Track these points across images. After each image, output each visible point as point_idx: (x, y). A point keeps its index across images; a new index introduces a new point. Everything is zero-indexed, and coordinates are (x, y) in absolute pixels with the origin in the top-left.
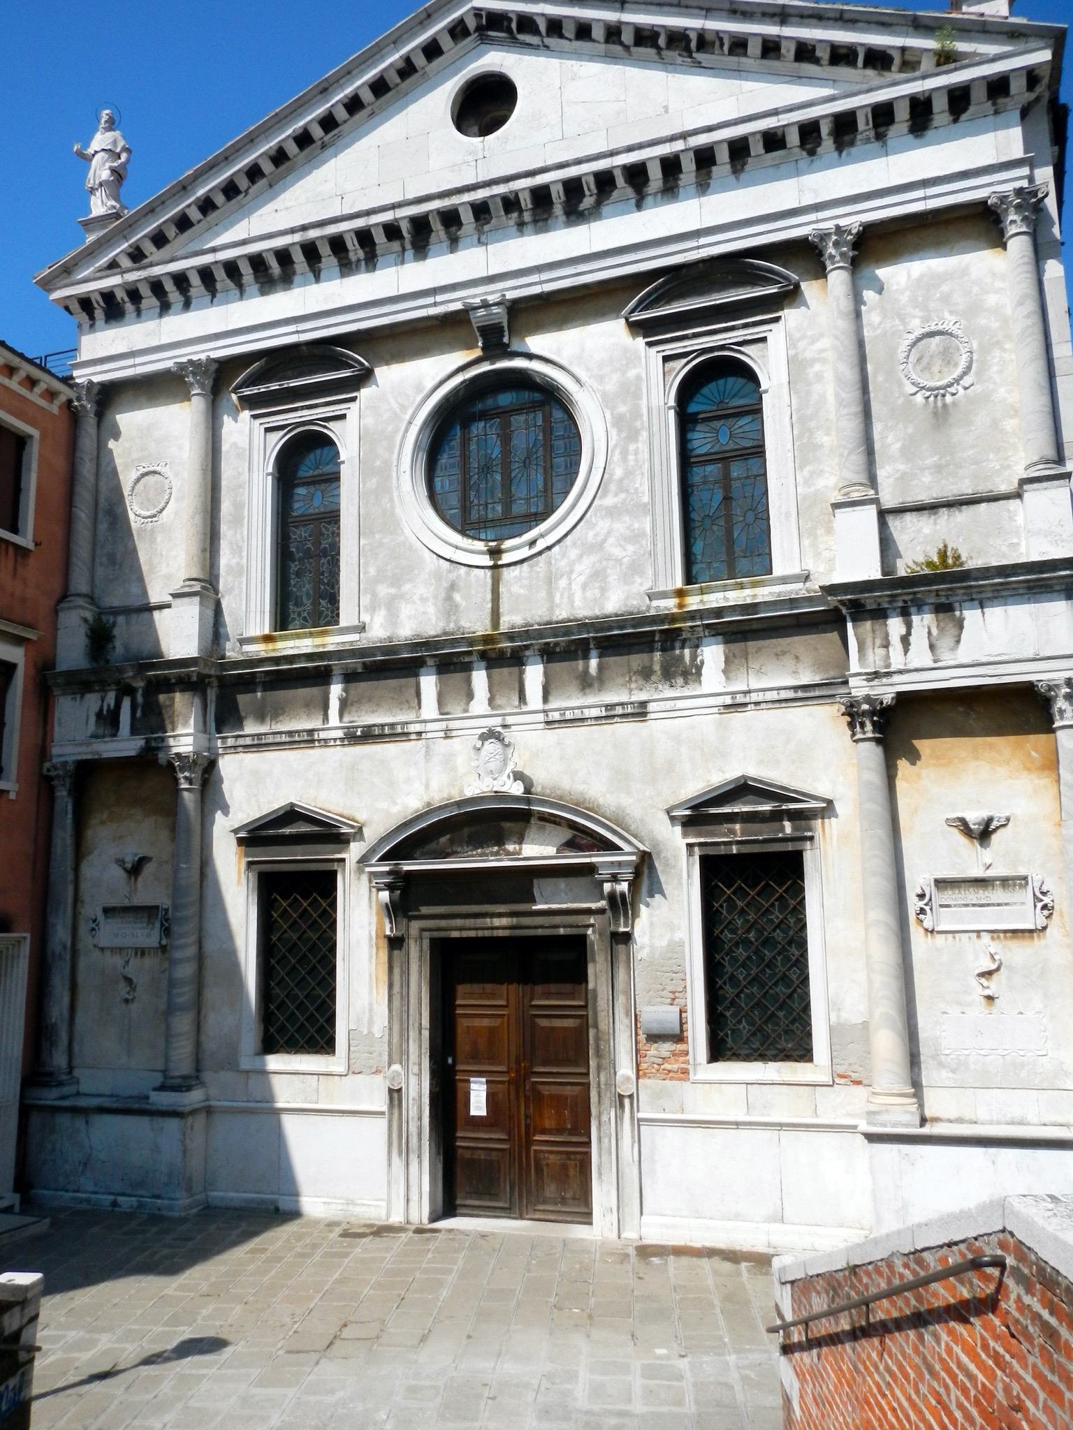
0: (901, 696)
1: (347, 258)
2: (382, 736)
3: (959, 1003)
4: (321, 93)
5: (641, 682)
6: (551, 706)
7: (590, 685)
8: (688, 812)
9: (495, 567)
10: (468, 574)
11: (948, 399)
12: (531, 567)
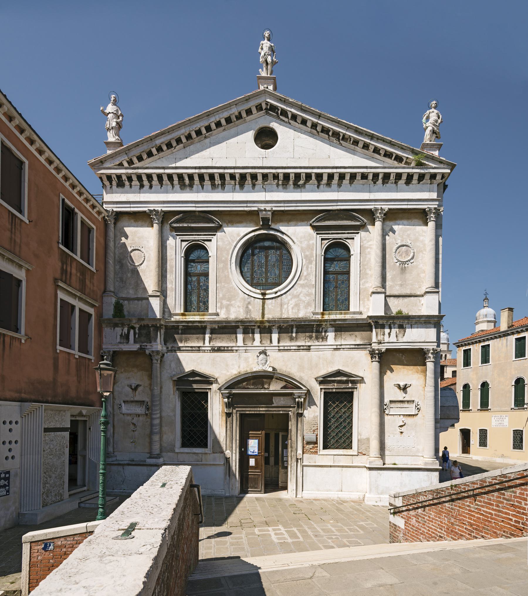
5: (309, 339)
6: (280, 345)
7: (293, 339)
9: (264, 299)
10: (254, 300)
11: (406, 265)
12: (275, 300)
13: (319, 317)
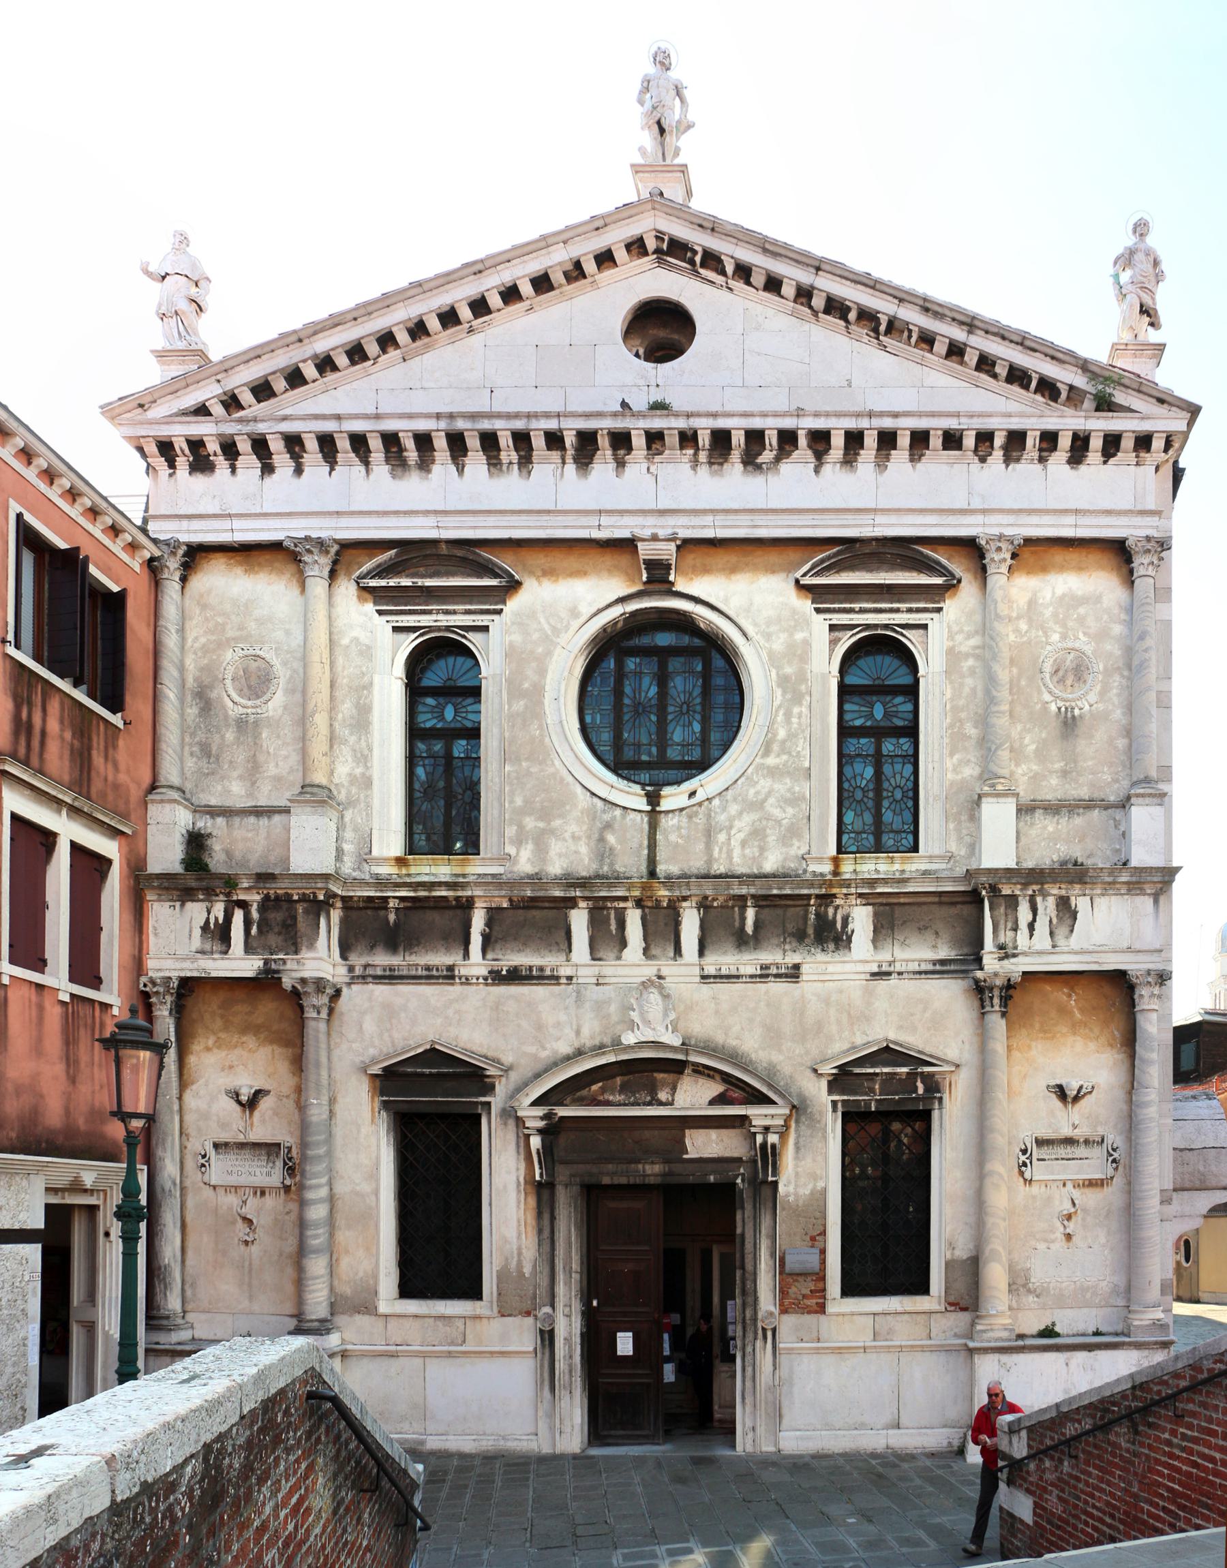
1: (497, 457)
8: (834, 1071)
13: (827, 868)
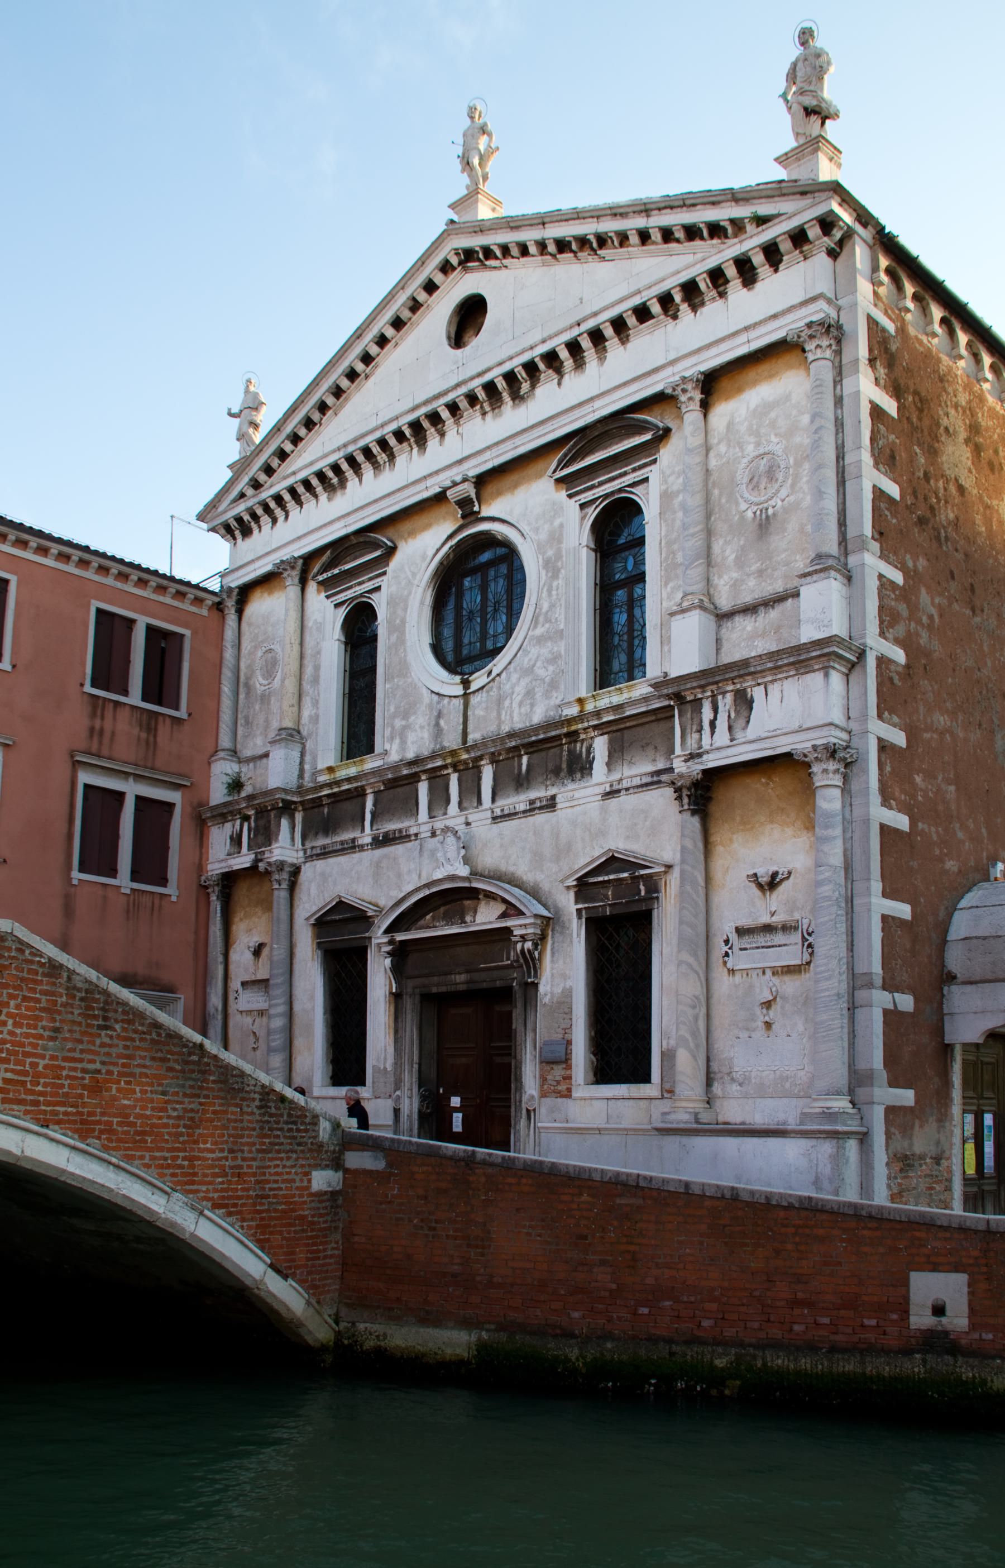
0: (705, 772)
1: (377, 462)
2: (394, 839)
3: (747, 1029)
4: (358, 338)
8: (575, 883)
9: (465, 694)
